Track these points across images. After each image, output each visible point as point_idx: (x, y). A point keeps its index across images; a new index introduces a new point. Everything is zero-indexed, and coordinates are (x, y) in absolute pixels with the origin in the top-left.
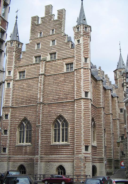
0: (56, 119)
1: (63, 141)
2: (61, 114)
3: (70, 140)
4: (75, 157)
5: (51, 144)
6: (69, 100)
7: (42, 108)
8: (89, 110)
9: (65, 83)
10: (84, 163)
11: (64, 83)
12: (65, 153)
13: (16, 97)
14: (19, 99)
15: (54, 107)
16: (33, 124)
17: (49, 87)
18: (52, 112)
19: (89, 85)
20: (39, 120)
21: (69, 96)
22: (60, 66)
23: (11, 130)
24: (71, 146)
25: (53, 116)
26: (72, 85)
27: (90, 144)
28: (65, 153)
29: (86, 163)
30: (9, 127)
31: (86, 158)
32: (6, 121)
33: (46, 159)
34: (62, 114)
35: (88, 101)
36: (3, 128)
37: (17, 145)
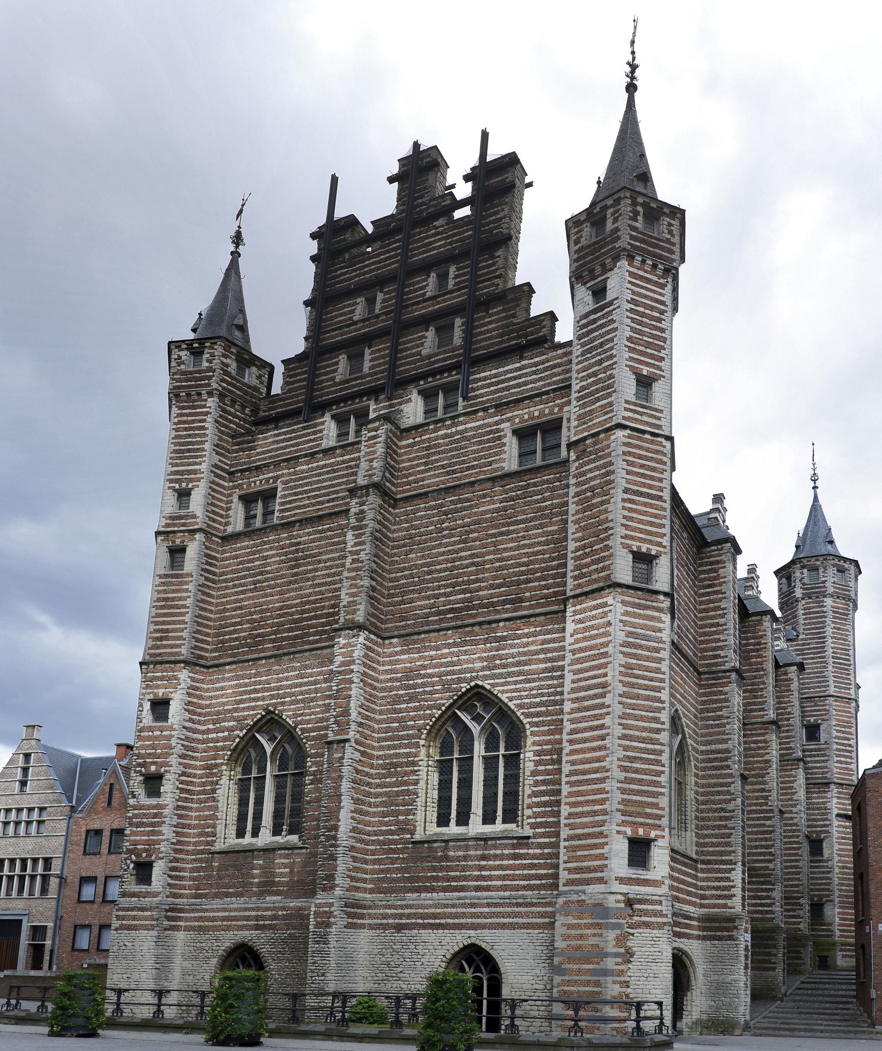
0: (448, 708)
1: (489, 818)
2: (480, 683)
3: (534, 813)
4: (561, 900)
5: (418, 837)
6: (531, 607)
7: (366, 656)
8: (658, 650)
9: (509, 524)
10: (618, 932)
11: (503, 525)
12: (500, 883)
13: (221, 619)
14: (239, 623)
15: (437, 648)
16: (314, 738)
17: (411, 551)
18: (424, 676)
19: (664, 521)
20: (346, 713)
21: (530, 590)
22: (480, 443)
23: (184, 774)
24: (541, 846)
25: (431, 693)
26: (552, 533)
27: (658, 833)
28: (500, 883)
29: (633, 934)
30: (173, 760)
31: (636, 906)
32: (157, 733)
33: (382, 911)
34: (487, 684)
35: (655, 604)
36: (140, 765)
37: (219, 846)
